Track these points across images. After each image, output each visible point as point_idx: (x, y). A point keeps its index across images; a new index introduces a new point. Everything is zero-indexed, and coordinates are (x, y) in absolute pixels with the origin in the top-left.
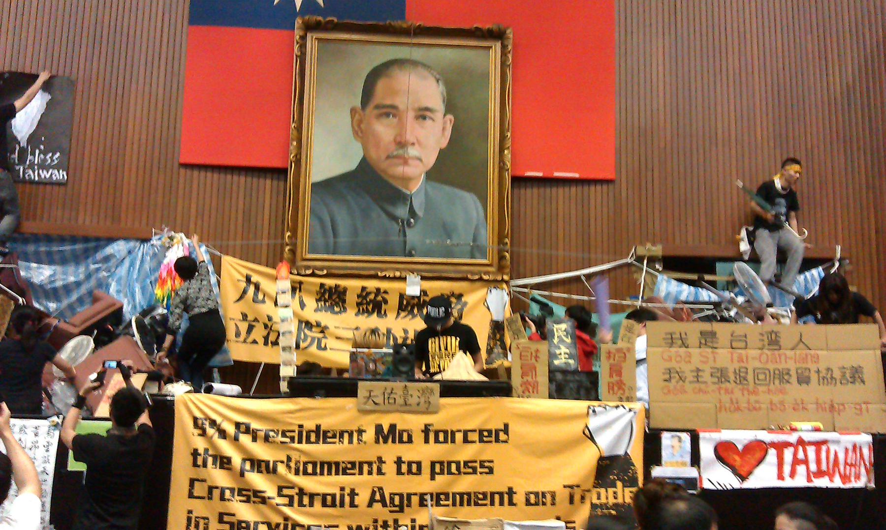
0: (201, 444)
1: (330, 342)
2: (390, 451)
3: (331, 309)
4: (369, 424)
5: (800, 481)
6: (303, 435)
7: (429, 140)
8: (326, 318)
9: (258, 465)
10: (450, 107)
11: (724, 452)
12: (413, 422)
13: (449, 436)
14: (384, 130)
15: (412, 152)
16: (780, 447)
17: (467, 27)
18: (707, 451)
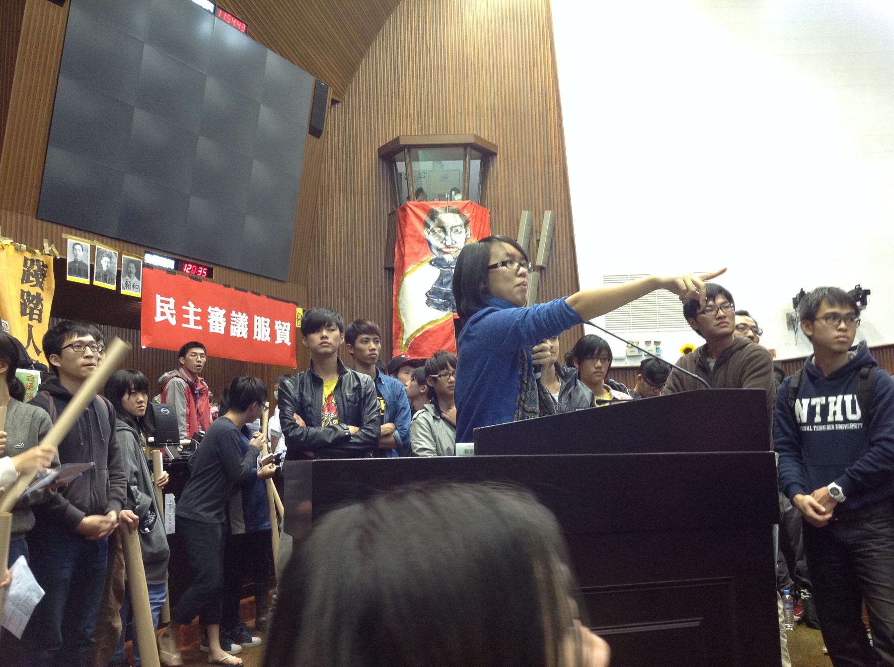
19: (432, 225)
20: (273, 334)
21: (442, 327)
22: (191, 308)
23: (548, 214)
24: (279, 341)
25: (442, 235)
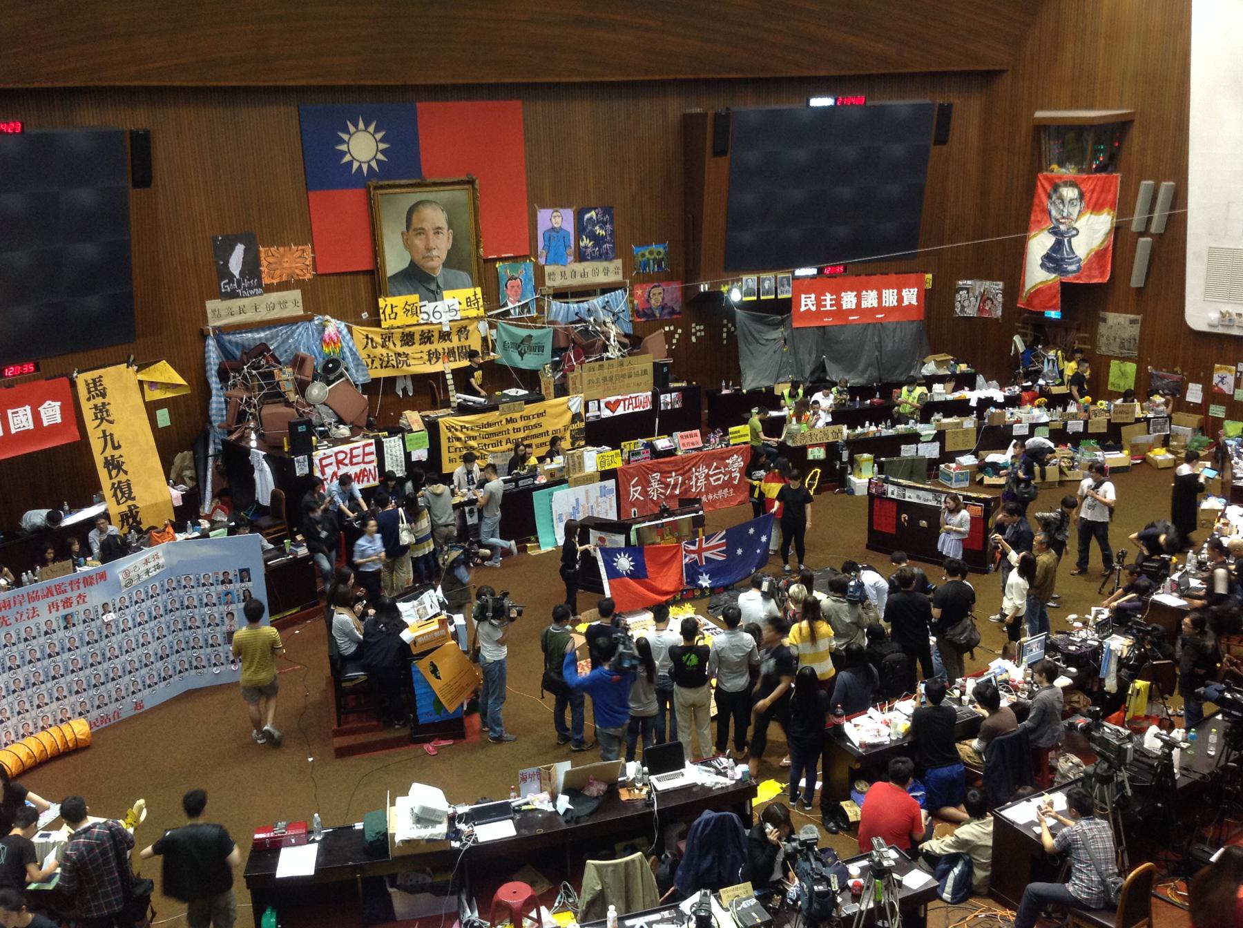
0: (450, 435)
1: (411, 361)
2: (511, 426)
3: (407, 344)
4: (503, 418)
5: (631, 411)
6: (484, 426)
7: (442, 245)
8: (406, 349)
9: (470, 438)
10: (450, 226)
11: (608, 405)
12: (517, 415)
13: (528, 418)
14: (419, 242)
15: (435, 253)
16: (624, 400)
17: (456, 179)
18: (602, 405)
19: (1054, 198)
20: (900, 299)
21: (1050, 288)
22: (828, 296)
23: (1167, 186)
24: (906, 303)
25: (1061, 206)
